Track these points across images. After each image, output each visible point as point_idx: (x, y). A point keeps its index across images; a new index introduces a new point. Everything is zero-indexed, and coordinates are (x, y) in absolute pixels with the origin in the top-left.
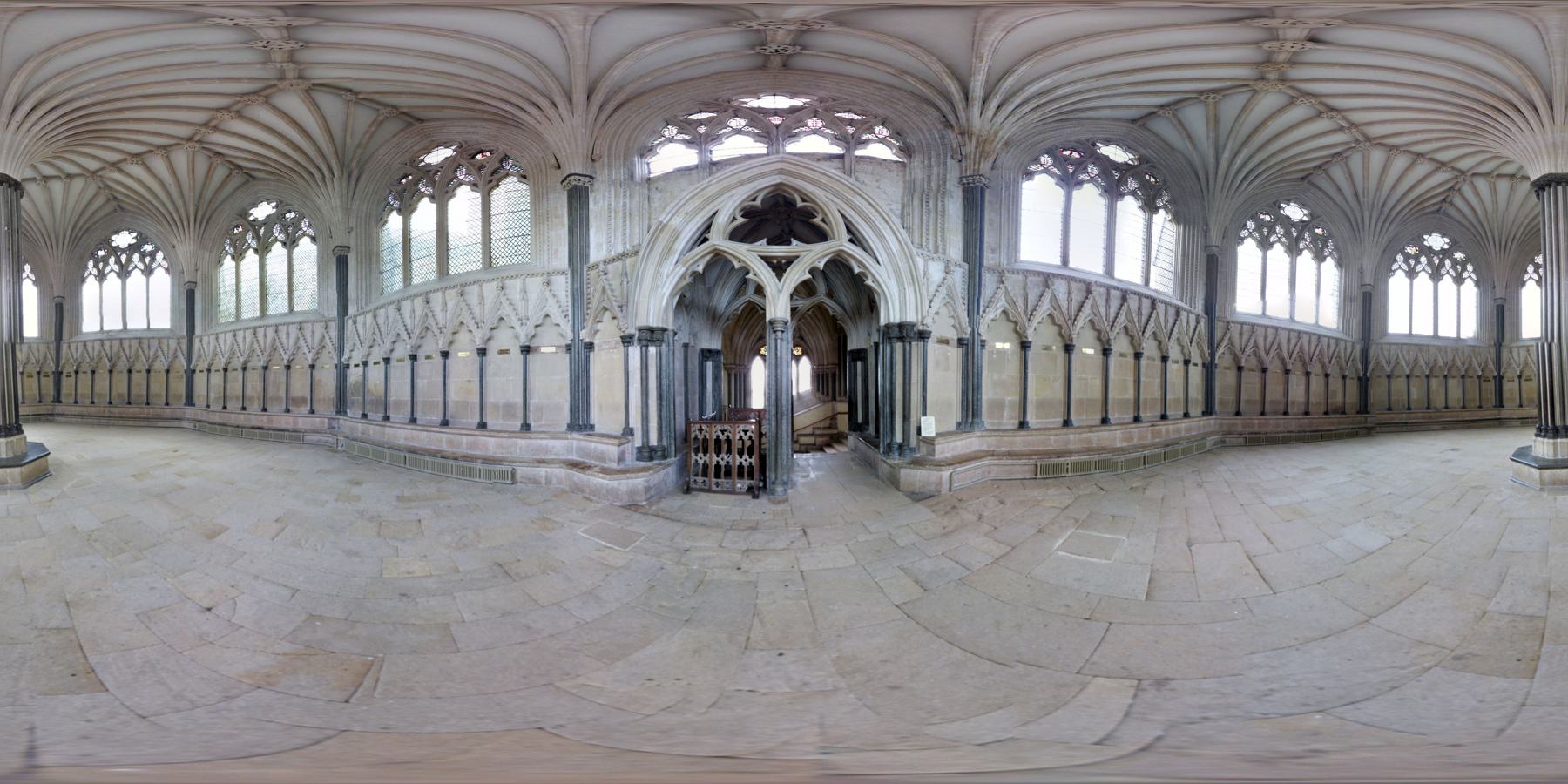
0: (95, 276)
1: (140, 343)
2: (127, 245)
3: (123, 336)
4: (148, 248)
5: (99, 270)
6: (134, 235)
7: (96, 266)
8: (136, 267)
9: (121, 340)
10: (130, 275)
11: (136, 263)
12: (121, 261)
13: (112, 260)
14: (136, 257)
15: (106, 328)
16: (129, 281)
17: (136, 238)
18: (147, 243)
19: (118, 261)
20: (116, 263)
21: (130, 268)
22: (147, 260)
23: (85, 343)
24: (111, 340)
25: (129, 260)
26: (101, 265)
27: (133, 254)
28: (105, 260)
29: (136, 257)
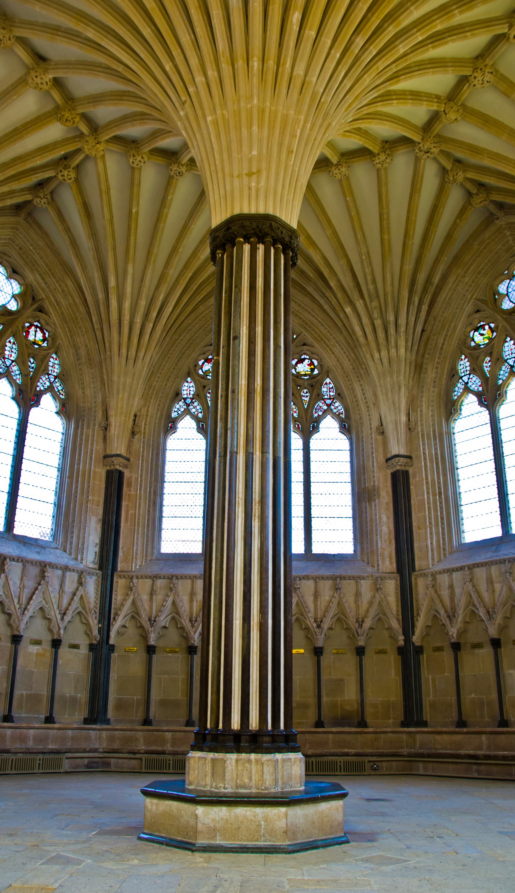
0: (478, 395)
5: (485, 380)
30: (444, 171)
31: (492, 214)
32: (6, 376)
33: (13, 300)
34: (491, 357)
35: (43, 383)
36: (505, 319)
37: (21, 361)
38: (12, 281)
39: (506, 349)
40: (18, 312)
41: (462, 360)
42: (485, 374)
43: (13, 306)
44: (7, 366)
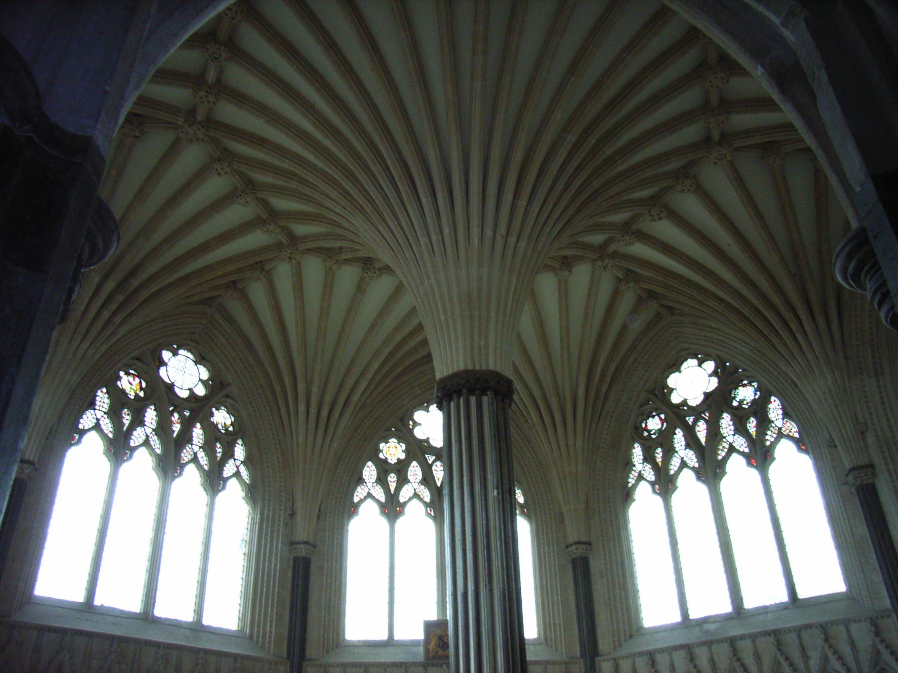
0: (653, 484)
1: (779, 645)
2: (701, 398)
3: (736, 631)
4: (746, 394)
6: (710, 366)
7: (649, 458)
8: (732, 449)
9: (732, 641)
10: (723, 473)
11: (730, 439)
12: (697, 440)
13: (679, 438)
14: (726, 423)
15: (695, 614)
16: (725, 485)
17: (715, 373)
18: (737, 384)
19: (692, 441)
20: (688, 446)
21: (722, 454)
22: (752, 425)
23: (651, 657)
24: (709, 644)
25: (715, 434)
26: (659, 454)
27: (719, 418)
28: (665, 440)
29: (726, 423)
30: (619, 280)
31: (659, 313)
32: (194, 463)
33: (200, 382)
34: (661, 447)
35: (229, 469)
36: (675, 414)
37: (208, 447)
38: (201, 368)
39: (676, 441)
40: (205, 397)
41: (634, 448)
42: (657, 464)
43: (201, 391)
44: (194, 453)
